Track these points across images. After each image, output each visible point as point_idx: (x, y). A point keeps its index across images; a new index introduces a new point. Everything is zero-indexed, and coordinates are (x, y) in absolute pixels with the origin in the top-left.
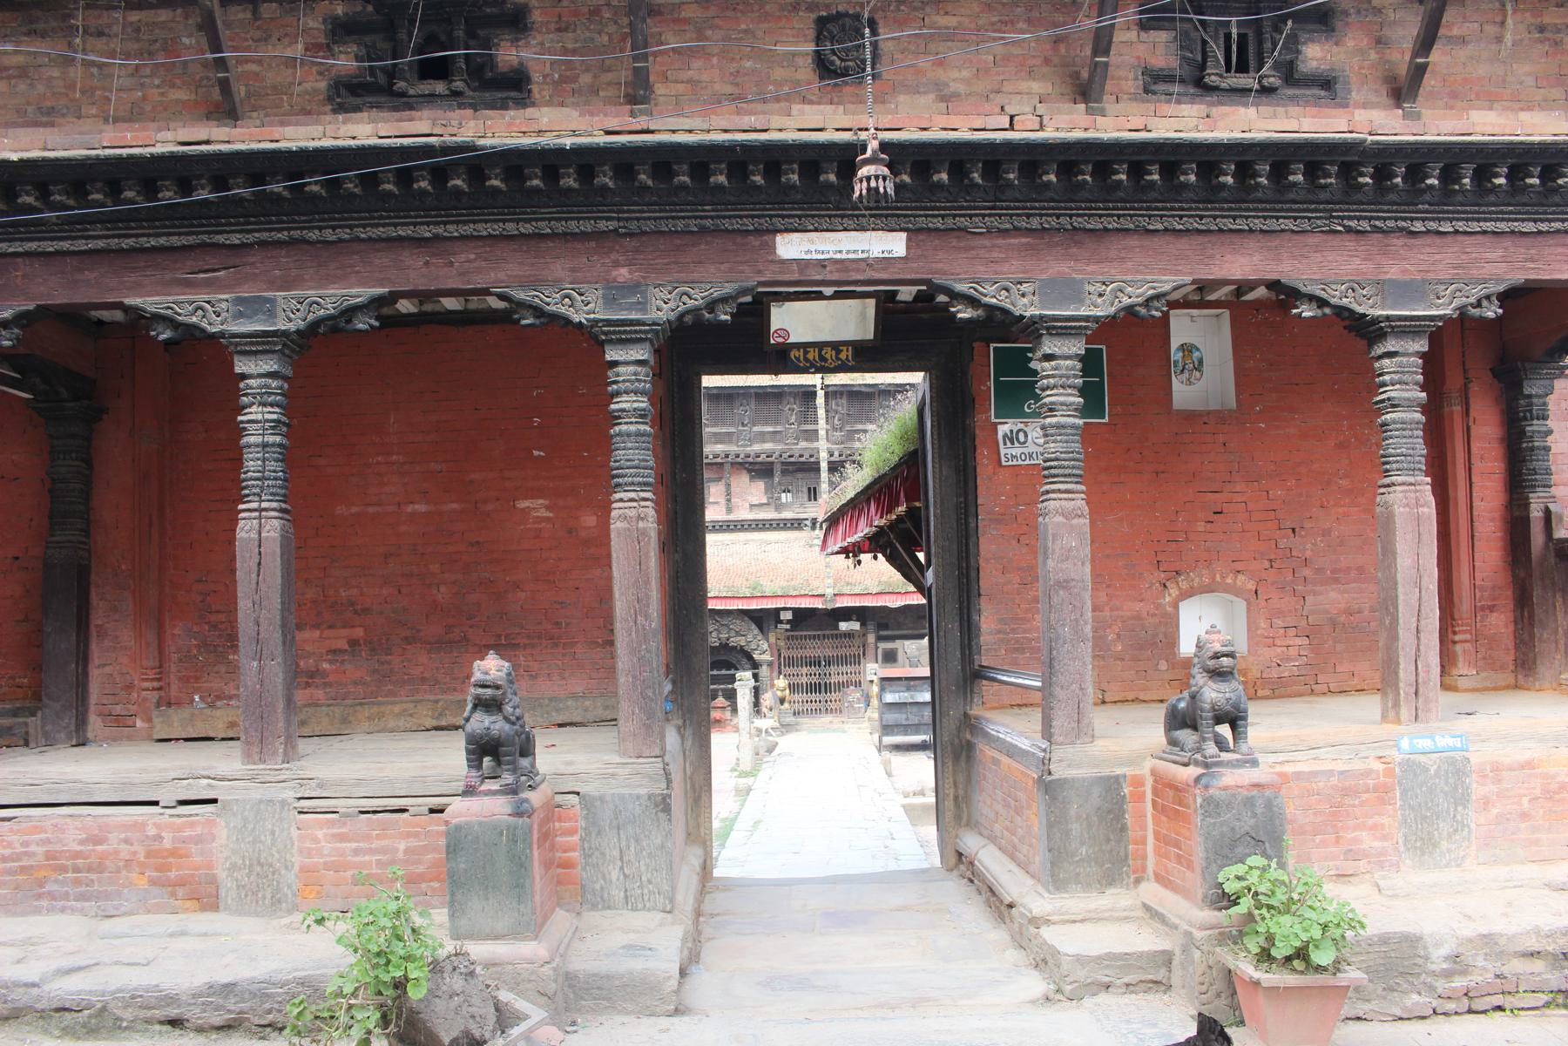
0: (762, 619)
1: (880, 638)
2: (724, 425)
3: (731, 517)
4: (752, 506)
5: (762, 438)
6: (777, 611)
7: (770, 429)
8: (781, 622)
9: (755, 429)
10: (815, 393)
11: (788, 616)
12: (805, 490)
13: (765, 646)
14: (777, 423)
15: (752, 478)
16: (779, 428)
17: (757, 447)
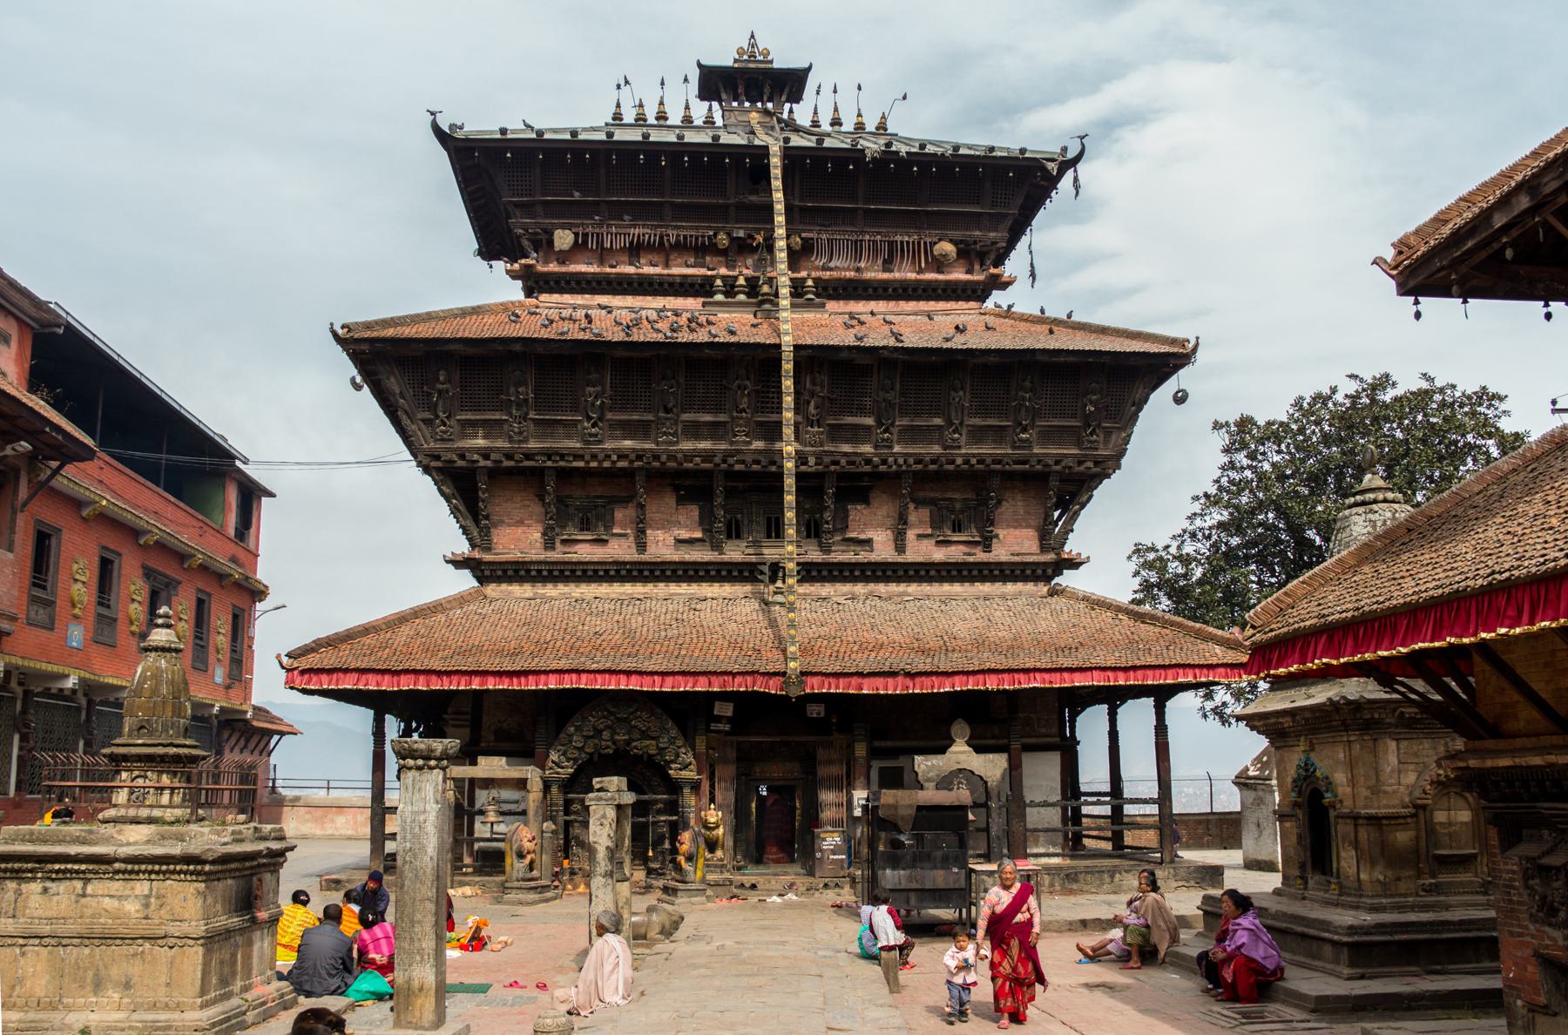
0: (686, 711)
1: (874, 753)
2: (635, 409)
3: (645, 557)
4: (679, 541)
5: (694, 431)
6: (710, 697)
7: (708, 418)
8: (719, 719)
9: (686, 417)
10: (777, 362)
11: (725, 710)
12: (762, 520)
13: (690, 758)
14: (718, 409)
15: (681, 501)
16: (722, 418)
17: (687, 445)
